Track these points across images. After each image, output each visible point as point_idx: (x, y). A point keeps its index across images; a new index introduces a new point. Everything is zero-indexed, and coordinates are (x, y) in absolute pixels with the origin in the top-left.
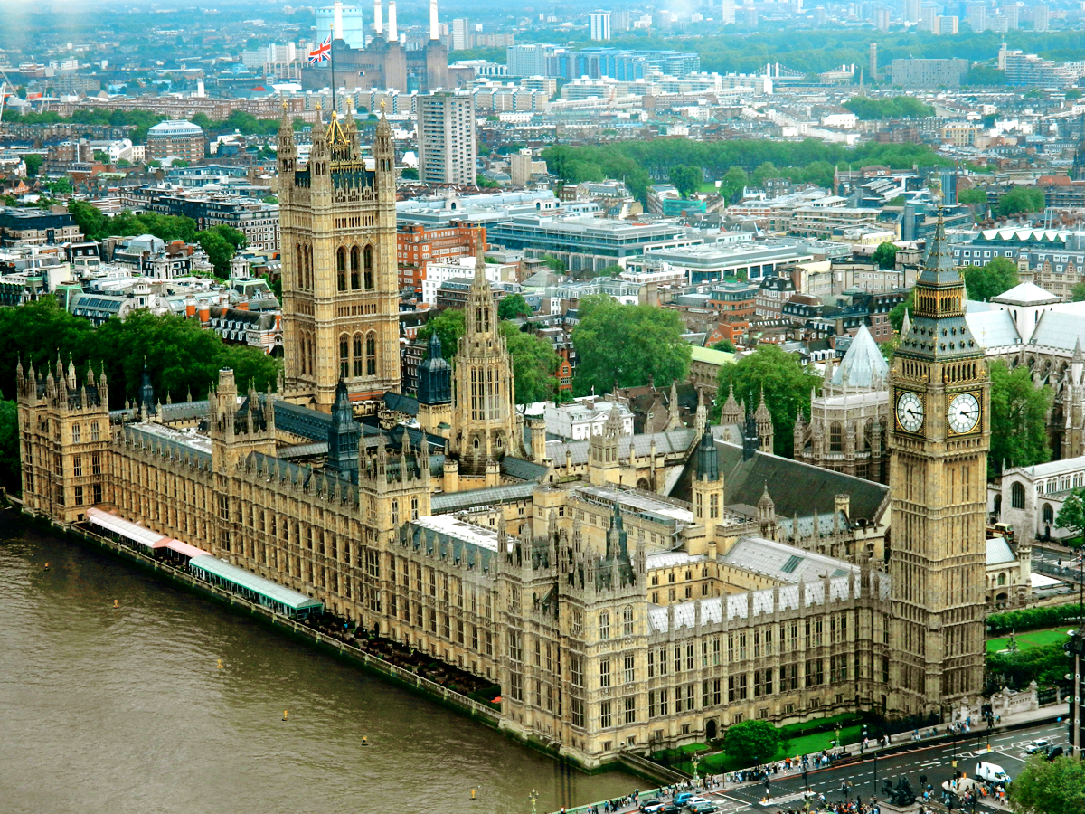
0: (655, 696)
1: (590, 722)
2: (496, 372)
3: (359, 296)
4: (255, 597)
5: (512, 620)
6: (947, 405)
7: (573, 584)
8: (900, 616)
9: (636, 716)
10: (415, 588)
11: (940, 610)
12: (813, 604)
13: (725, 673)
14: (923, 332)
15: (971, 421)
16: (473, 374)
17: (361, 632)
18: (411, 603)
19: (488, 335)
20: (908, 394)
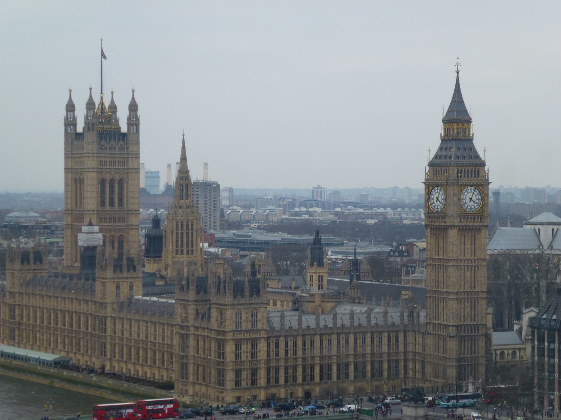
0: (271, 370)
1: (228, 382)
2: (192, 225)
3: (114, 211)
4: (27, 359)
5: (182, 327)
6: (461, 192)
7: (220, 295)
8: (432, 332)
9: (258, 382)
10: (128, 336)
11: (457, 324)
12: (377, 324)
13: (317, 361)
14: (446, 149)
15: (476, 205)
16: (177, 225)
17: (92, 371)
18: (125, 346)
19: (187, 201)
20: (435, 188)
